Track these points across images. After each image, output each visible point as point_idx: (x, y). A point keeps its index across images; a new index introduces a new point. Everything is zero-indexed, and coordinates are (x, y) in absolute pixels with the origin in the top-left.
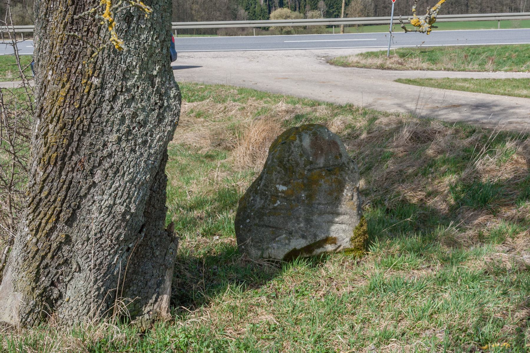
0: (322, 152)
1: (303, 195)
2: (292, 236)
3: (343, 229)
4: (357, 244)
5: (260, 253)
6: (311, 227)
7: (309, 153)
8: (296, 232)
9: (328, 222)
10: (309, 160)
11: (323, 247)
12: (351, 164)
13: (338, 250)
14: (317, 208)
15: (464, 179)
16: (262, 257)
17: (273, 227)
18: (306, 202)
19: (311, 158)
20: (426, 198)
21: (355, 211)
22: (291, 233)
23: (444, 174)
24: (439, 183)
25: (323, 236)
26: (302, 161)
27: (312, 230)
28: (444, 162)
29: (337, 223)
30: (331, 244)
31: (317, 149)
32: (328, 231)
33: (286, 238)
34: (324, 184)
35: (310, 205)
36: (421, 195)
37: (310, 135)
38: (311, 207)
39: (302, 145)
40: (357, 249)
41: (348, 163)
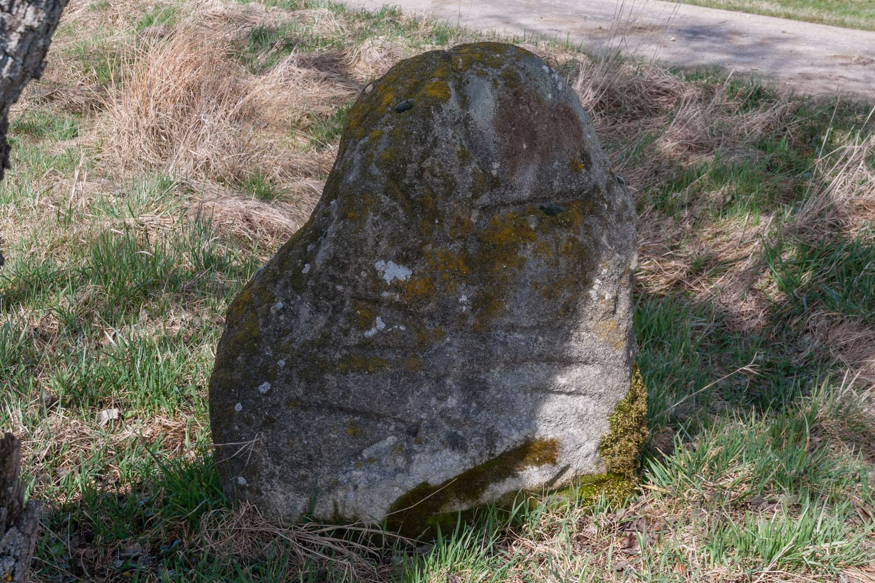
0: (532, 146)
1: (464, 298)
2: (419, 442)
3: (578, 413)
4: (618, 460)
5: (302, 503)
6: (481, 406)
7: (492, 148)
8: (433, 426)
9: (536, 389)
10: (487, 174)
11: (515, 476)
12: (617, 189)
13: (558, 483)
14: (504, 343)
15: (802, 231)
16: (308, 515)
17: (355, 412)
18: (471, 321)
19: (496, 165)
20: (691, 280)
21: (620, 353)
22: (413, 432)
23: (725, 207)
24: (716, 235)
25: (515, 437)
26: (465, 178)
27: (483, 416)
28: (719, 176)
29: (560, 393)
30: (539, 464)
31: (516, 133)
32: (532, 417)
33: (395, 449)
34: (534, 261)
35: (483, 333)
36: (676, 268)
37: (495, 83)
38: (484, 340)
39: (468, 117)
40: (617, 475)
41: (609, 189)
